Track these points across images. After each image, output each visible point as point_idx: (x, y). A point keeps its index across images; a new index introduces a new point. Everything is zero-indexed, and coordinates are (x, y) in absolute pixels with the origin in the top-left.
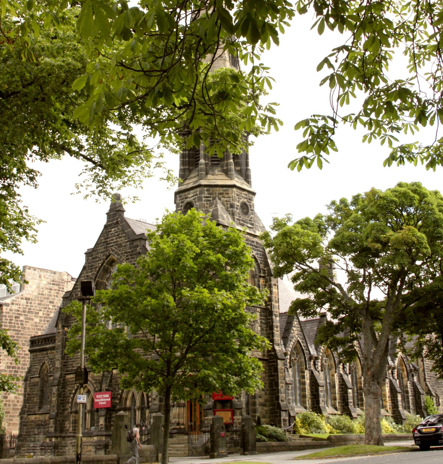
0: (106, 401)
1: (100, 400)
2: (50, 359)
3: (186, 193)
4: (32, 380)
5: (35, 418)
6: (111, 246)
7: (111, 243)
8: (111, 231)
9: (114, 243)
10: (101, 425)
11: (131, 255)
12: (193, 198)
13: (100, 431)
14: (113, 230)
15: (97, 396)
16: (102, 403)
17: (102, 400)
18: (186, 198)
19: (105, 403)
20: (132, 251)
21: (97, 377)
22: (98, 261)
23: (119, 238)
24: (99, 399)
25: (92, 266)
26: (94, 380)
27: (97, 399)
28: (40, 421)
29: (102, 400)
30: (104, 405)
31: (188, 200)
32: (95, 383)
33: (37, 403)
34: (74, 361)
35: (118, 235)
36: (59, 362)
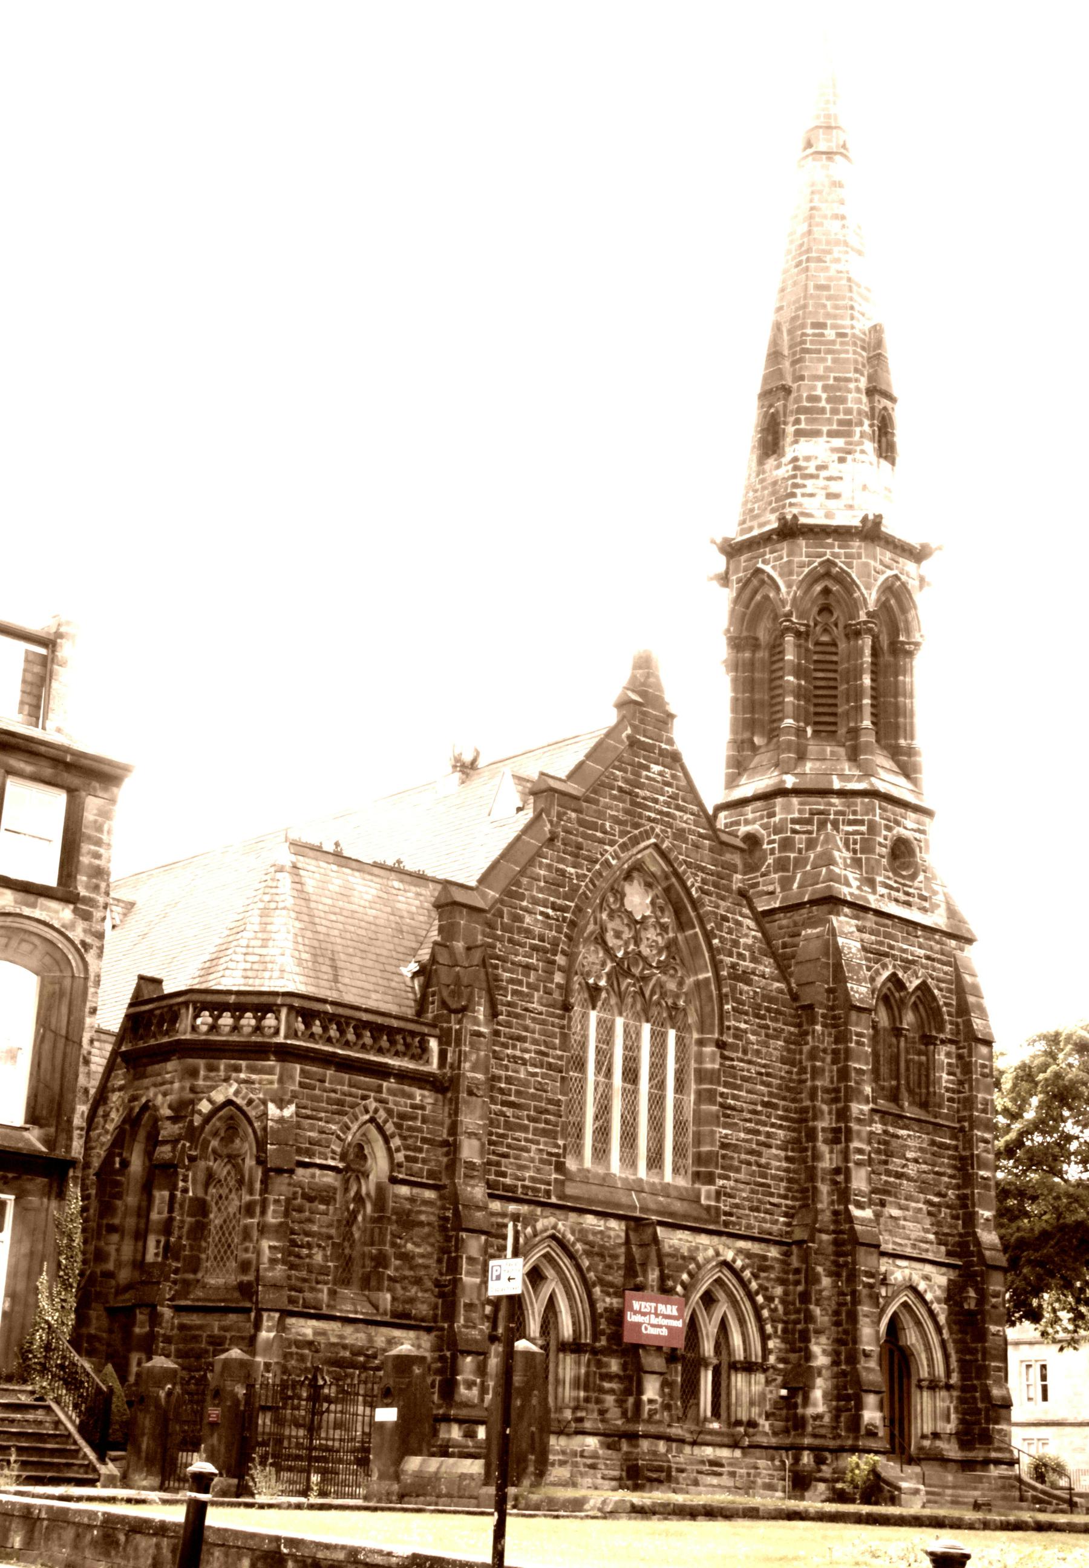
0: (667, 1327)
1: (646, 1319)
2: (390, 1112)
3: (899, 810)
4: (300, 1171)
5: (316, 1333)
6: (649, 819)
7: (649, 809)
8: (648, 769)
9: (660, 813)
10: (651, 1401)
11: (716, 885)
12: (918, 835)
13: (649, 1421)
14: (656, 768)
15: (636, 1305)
16: (652, 1331)
17: (654, 1320)
18: (898, 823)
19: (664, 1332)
20: (719, 876)
21: (595, 1233)
22: (601, 842)
23: (678, 808)
24: (644, 1314)
25: (579, 847)
26: (586, 1243)
27: (636, 1313)
28: (345, 1347)
29: (654, 1320)
30: (658, 1337)
31: (898, 831)
32: (588, 1254)
33: (324, 1271)
34: (506, 1156)
35: (674, 797)
36: (475, 1143)
